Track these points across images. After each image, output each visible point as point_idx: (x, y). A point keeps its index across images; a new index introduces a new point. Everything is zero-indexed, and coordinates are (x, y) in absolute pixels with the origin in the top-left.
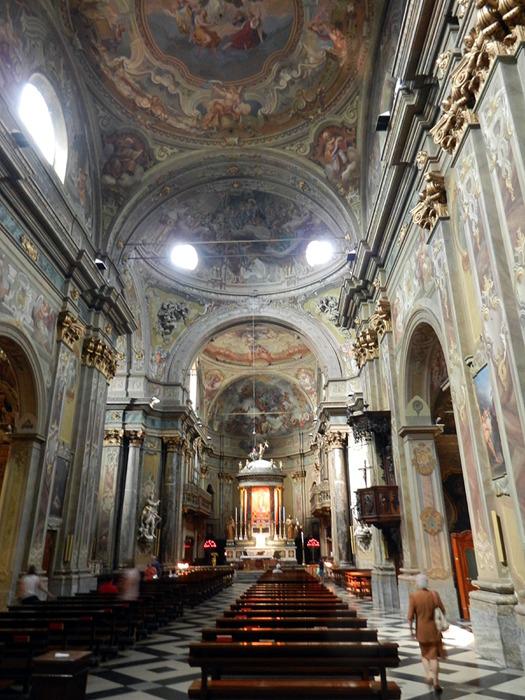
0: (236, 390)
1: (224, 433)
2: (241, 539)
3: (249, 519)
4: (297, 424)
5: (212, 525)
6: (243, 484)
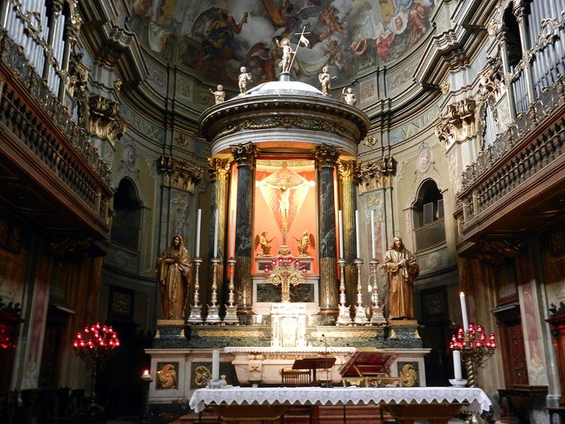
2: (214, 317)
3: (245, 251)
4: (370, 50)
5: (130, 293)
6: (226, 143)
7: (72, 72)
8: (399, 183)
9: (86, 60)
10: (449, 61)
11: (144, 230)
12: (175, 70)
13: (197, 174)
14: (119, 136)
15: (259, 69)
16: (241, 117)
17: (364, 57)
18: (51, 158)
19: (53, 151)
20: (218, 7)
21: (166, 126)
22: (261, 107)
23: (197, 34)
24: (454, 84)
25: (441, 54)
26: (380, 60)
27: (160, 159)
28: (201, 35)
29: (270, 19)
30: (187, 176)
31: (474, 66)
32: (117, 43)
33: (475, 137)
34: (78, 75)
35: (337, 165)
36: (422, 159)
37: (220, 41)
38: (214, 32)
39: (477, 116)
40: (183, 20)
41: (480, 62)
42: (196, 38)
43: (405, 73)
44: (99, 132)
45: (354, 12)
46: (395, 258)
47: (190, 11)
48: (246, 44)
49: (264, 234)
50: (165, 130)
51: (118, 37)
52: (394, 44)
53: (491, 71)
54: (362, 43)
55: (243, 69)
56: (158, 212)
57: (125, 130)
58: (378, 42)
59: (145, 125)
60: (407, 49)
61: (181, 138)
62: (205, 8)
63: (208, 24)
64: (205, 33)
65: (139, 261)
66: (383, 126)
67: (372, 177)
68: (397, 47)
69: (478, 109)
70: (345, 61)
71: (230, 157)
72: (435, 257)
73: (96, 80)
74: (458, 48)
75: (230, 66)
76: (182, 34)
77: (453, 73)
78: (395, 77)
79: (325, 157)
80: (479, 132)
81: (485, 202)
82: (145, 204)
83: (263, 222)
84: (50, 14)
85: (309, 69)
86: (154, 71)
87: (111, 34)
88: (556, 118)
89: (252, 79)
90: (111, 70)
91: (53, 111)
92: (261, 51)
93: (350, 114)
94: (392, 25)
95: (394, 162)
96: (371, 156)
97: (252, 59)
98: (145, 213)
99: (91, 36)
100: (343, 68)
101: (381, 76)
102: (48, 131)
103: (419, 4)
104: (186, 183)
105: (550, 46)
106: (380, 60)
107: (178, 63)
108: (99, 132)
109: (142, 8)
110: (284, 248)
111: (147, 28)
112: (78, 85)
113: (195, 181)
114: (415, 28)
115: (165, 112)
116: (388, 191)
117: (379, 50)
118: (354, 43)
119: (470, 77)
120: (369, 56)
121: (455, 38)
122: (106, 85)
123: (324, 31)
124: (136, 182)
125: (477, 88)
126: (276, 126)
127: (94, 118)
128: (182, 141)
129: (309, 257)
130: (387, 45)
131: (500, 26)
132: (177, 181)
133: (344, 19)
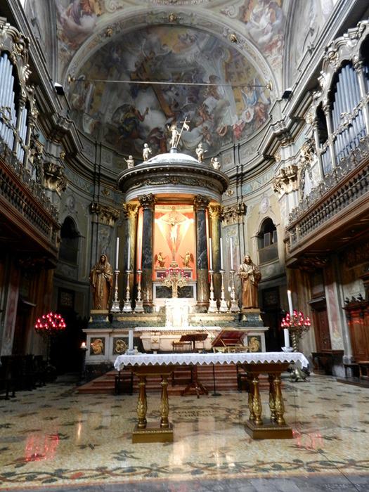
0: (124, 64)
1: (103, 141)
2: (128, 308)
3: (148, 266)
4: (229, 133)
5: (72, 292)
6: (135, 194)
7: (32, 146)
8: (248, 220)
9: (41, 139)
10: (280, 140)
11: (81, 252)
12: (101, 145)
13: (115, 214)
14: (64, 189)
15: (156, 145)
16: (145, 177)
17: (225, 138)
18: (19, 204)
19: (20, 199)
20: (127, 103)
21: (94, 183)
22: (158, 171)
23: (115, 122)
24: (284, 156)
25: (275, 136)
26: (236, 139)
27: (91, 205)
28: (118, 123)
29: (163, 111)
30: (109, 215)
31: (296, 144)
32: (62, 128)
33: (297, 190)
34: (37, 150)
35: (208, 209)
36: (263, 205)
37: (130, 126)
38: (126, 120)
39: (298, 176)
40: (105, 112)
41: (301, 140)
42: (114, 124)
43: (252, 148)
44: (50, 187)
45: (218, 108)
46: (246, 269)
47: (110, 107)
48: (147, 128)
49: (160, 254)
50: (94, 185)
51: (62, 123)
52: (244, 129)
53: (308, 147)
54: (224, 128)
55: (146, 145)
56: (90, 239)
57: (68, 185)
58: (234, 128)
59: (82, 182)
60: (253, 132)
61: (105, 191)
62: (120, 104)
63: (122, 115)
64: (121, 122)
65: (78, 270)
66: (237, 183)
67: (231, 216)
68: (246, 131)
69: (299, 172)
70: (212, 140)
71: (138, 203)
72: (271, 268)
73: (48, 151)
74: (286, 132)
75: (137, 143)
76: (105, 121)
77: (283, 148)
78: (245, 151)
79: (200, 203)
80: (300, 187)
81: (304, 232)
82: (81, 234)
83: (160, 246)
84: (17, 108)
85: (189, 146)
86: (86, 146)
87: (58, 122)
88: (350, 178)
89: (152, 152)
90: (58, 146)
91: (20, 173)
92: (158, 133)
93: (216, 175)
94: (244, 117)
95: (245, 206)
96: (231, 203)
97: (152, 138)
98: (81, 240)
99: (44, 123)
100: (211, 145)
101: (237, 150)
102: (17, 186)
103: (261, 103)
104: (109, 220)
105: (346, 131)
106: (236, 139)
107: (103, 141)
108: (50, 187)
109: (78, 104)
110: (174, 263)
111: (81, 118)
112: (36, 155)
113: (115, 219)
114: (258, 119)
115: (94, 174)
116: (241, 225)
117: (235, 133)
118: (218, 129)
119: (294, 151)
120: (228, 137)
121: (284, 125)
122: (55, 155)
123: (199, 120)
124: (76, 220)
125: (299, 158)
126: (168, 183)
127: (47, 177)
128: (106, 193)
129: (190, 269)
130: (240, 130)
131: (314, 117)
132: (102, 219)
133: (212, 111)
